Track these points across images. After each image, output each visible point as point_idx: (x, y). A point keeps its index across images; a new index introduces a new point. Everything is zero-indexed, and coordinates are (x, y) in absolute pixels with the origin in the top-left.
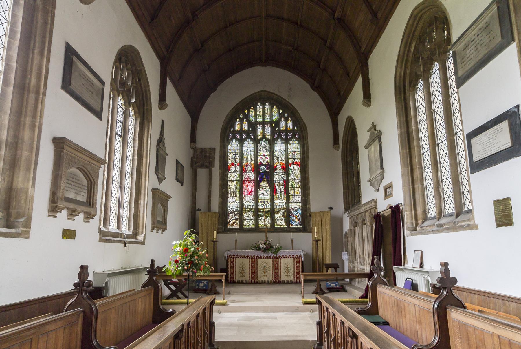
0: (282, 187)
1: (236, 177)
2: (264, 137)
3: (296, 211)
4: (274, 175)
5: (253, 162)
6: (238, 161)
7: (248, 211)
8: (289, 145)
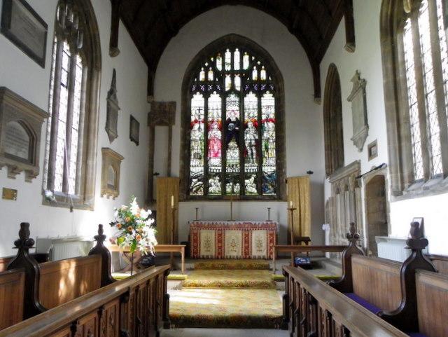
0: (253, 148)
6: (202, 117)
7: (215, 176)
8: (262, 98)
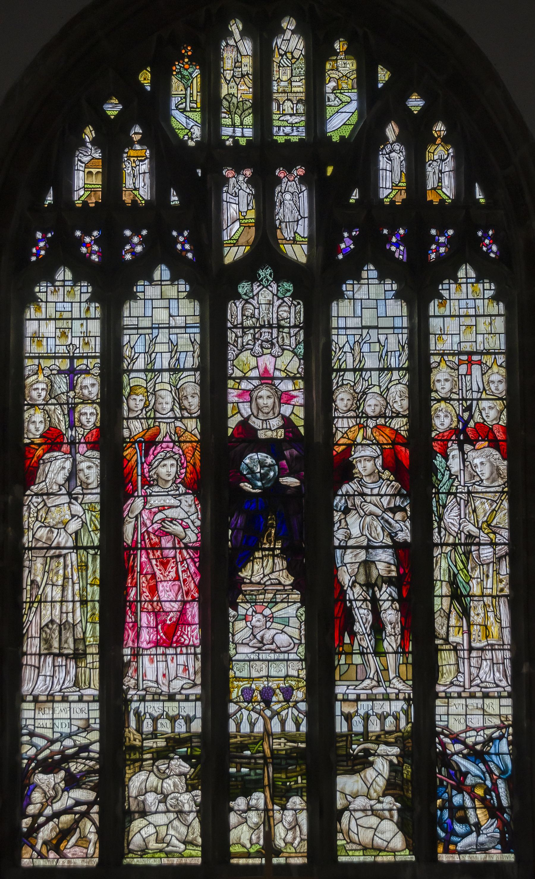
0: (386, 593)
1: (74, 526)
2: (265, 250)
3: (477, 755)
4: (330, 509)
5: (192, 425)
6: (89, 416)
7: (161, 754)
8: (433, 308)
